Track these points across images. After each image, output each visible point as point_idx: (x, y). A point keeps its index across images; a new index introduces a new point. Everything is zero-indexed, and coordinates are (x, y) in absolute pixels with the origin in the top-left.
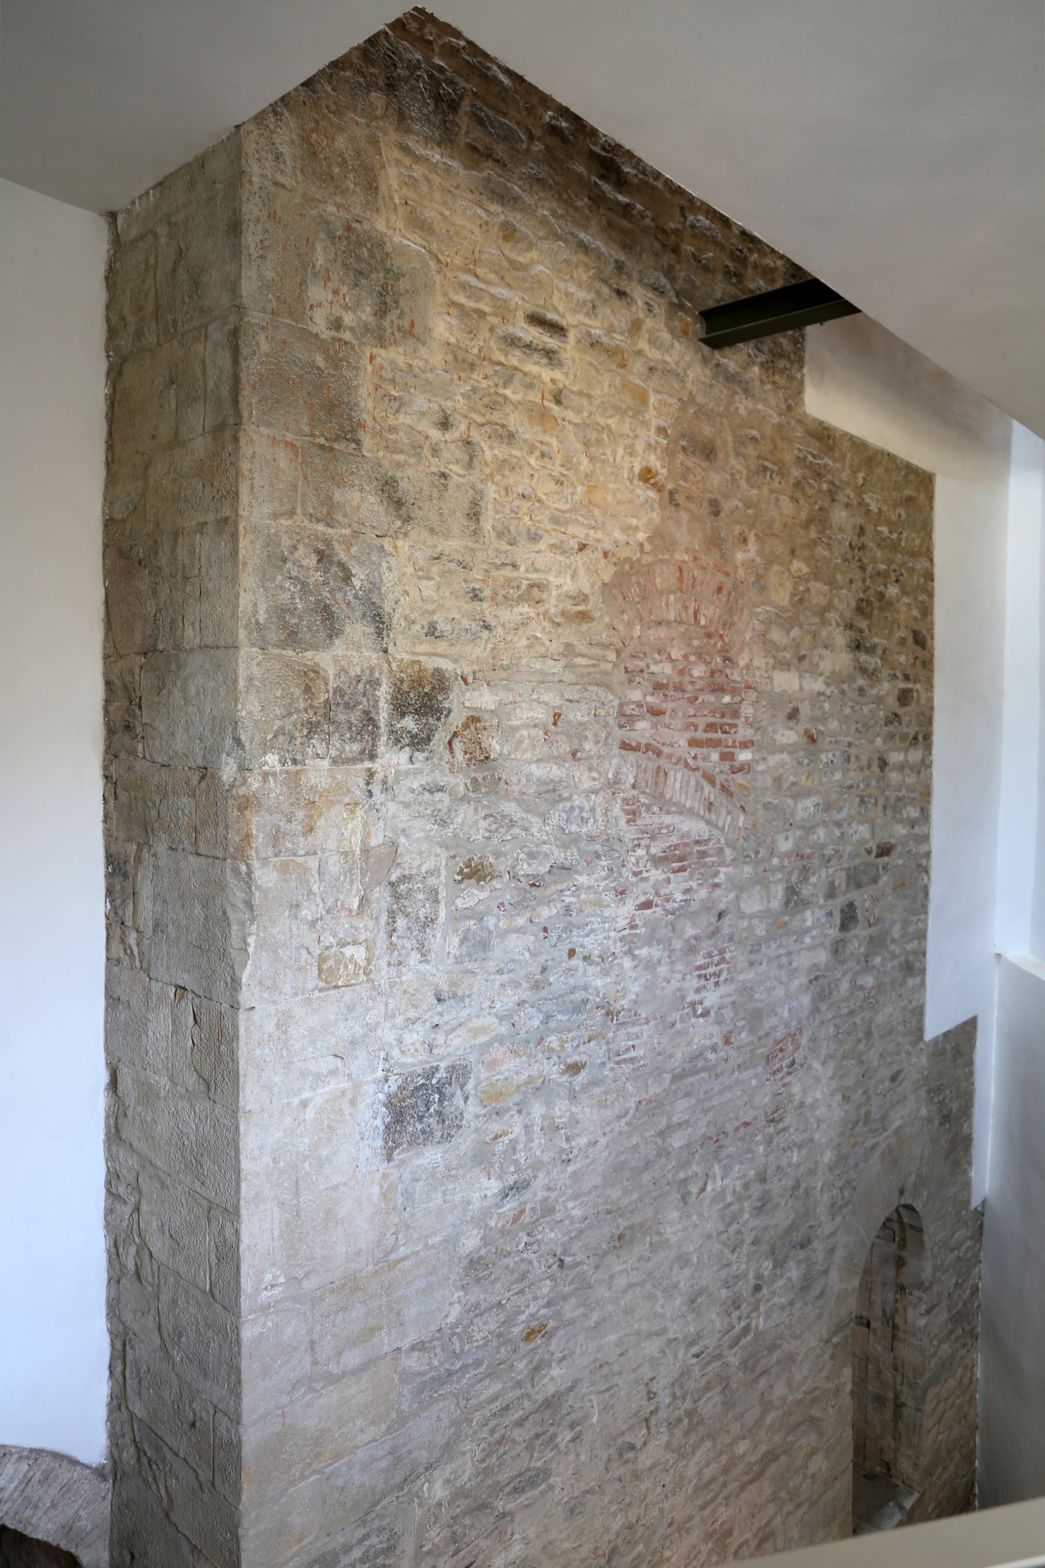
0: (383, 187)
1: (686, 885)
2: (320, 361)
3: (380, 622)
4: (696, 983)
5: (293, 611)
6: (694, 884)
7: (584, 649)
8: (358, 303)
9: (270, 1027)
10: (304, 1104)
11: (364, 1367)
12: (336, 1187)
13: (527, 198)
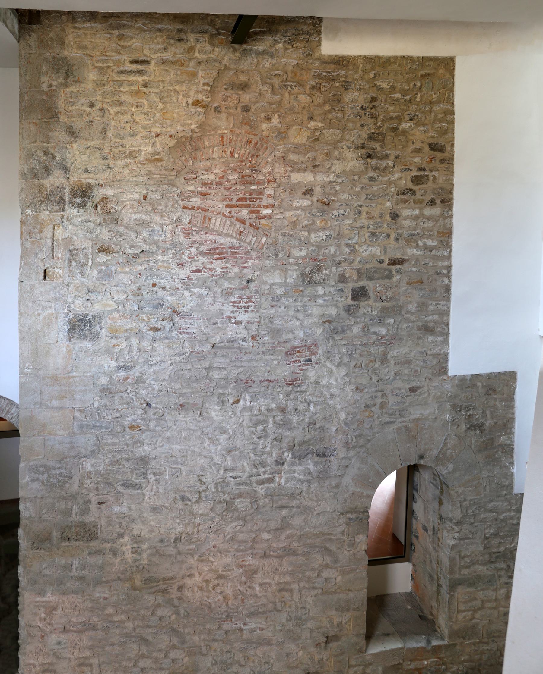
0: (67, 41)
1: (224, 266)
2: (45, 97)
3: (65, 170)
4: (231, 308)
5: (36, 169)
6: (229, 266)
7: (157, 172)
8: (58, 78)
9: (28, 288)
10: (39, 314)
11: (60, 408)
12: (50, 344)
13: (130, 23)
